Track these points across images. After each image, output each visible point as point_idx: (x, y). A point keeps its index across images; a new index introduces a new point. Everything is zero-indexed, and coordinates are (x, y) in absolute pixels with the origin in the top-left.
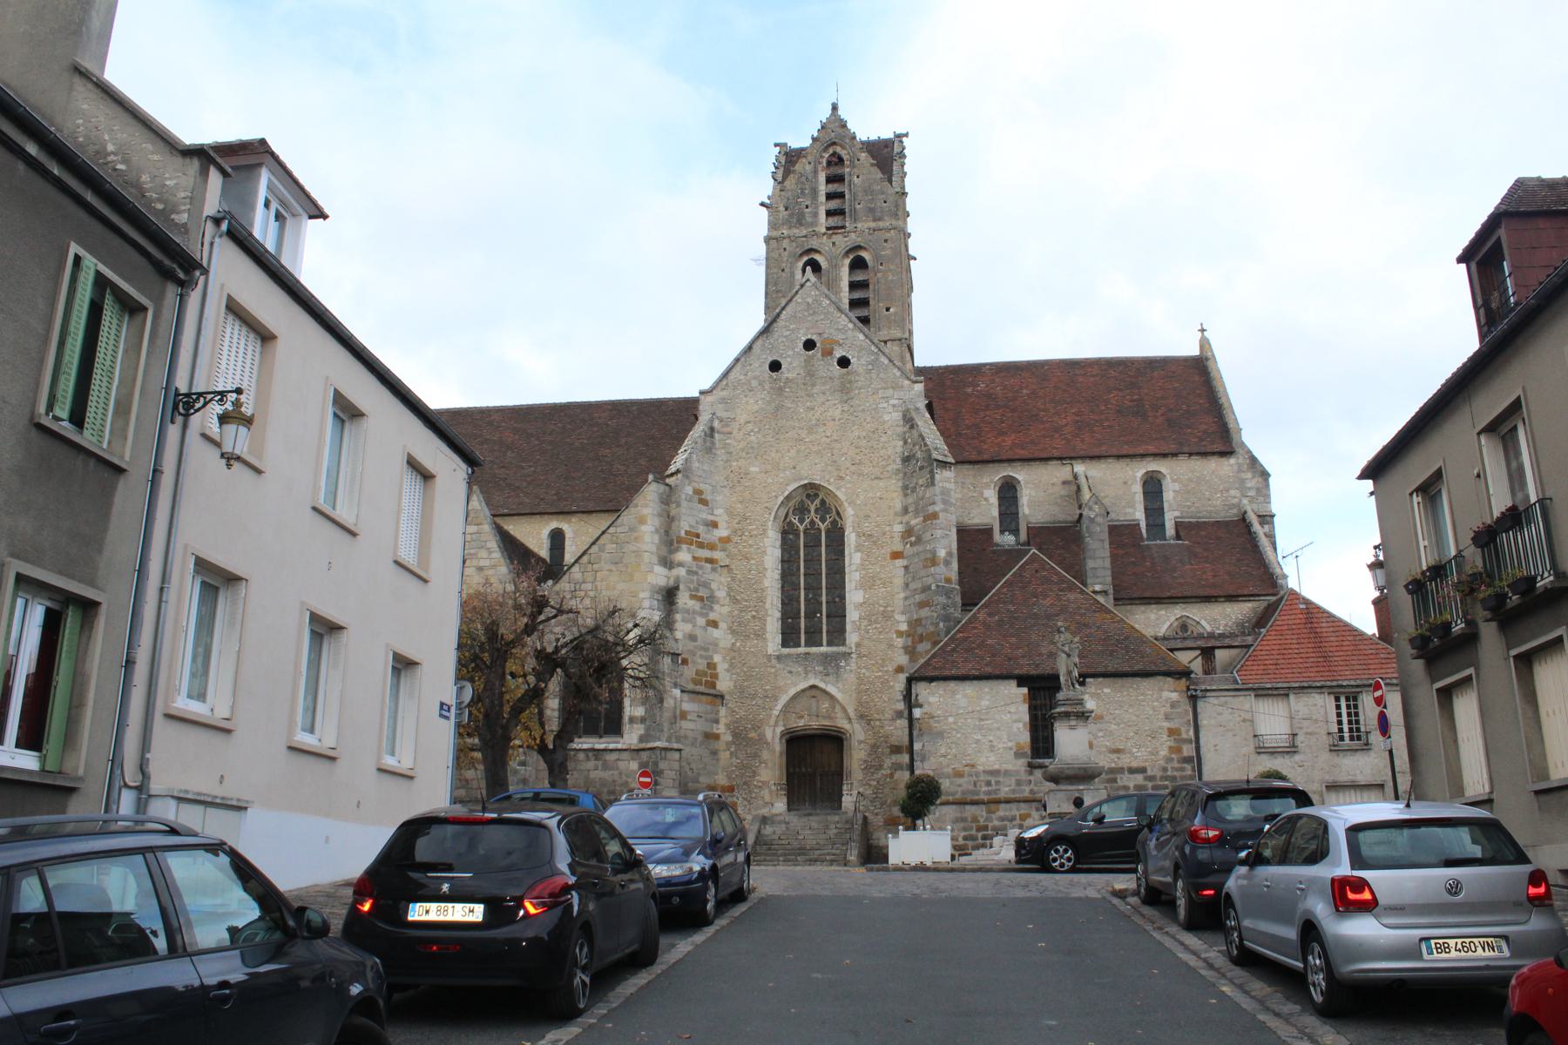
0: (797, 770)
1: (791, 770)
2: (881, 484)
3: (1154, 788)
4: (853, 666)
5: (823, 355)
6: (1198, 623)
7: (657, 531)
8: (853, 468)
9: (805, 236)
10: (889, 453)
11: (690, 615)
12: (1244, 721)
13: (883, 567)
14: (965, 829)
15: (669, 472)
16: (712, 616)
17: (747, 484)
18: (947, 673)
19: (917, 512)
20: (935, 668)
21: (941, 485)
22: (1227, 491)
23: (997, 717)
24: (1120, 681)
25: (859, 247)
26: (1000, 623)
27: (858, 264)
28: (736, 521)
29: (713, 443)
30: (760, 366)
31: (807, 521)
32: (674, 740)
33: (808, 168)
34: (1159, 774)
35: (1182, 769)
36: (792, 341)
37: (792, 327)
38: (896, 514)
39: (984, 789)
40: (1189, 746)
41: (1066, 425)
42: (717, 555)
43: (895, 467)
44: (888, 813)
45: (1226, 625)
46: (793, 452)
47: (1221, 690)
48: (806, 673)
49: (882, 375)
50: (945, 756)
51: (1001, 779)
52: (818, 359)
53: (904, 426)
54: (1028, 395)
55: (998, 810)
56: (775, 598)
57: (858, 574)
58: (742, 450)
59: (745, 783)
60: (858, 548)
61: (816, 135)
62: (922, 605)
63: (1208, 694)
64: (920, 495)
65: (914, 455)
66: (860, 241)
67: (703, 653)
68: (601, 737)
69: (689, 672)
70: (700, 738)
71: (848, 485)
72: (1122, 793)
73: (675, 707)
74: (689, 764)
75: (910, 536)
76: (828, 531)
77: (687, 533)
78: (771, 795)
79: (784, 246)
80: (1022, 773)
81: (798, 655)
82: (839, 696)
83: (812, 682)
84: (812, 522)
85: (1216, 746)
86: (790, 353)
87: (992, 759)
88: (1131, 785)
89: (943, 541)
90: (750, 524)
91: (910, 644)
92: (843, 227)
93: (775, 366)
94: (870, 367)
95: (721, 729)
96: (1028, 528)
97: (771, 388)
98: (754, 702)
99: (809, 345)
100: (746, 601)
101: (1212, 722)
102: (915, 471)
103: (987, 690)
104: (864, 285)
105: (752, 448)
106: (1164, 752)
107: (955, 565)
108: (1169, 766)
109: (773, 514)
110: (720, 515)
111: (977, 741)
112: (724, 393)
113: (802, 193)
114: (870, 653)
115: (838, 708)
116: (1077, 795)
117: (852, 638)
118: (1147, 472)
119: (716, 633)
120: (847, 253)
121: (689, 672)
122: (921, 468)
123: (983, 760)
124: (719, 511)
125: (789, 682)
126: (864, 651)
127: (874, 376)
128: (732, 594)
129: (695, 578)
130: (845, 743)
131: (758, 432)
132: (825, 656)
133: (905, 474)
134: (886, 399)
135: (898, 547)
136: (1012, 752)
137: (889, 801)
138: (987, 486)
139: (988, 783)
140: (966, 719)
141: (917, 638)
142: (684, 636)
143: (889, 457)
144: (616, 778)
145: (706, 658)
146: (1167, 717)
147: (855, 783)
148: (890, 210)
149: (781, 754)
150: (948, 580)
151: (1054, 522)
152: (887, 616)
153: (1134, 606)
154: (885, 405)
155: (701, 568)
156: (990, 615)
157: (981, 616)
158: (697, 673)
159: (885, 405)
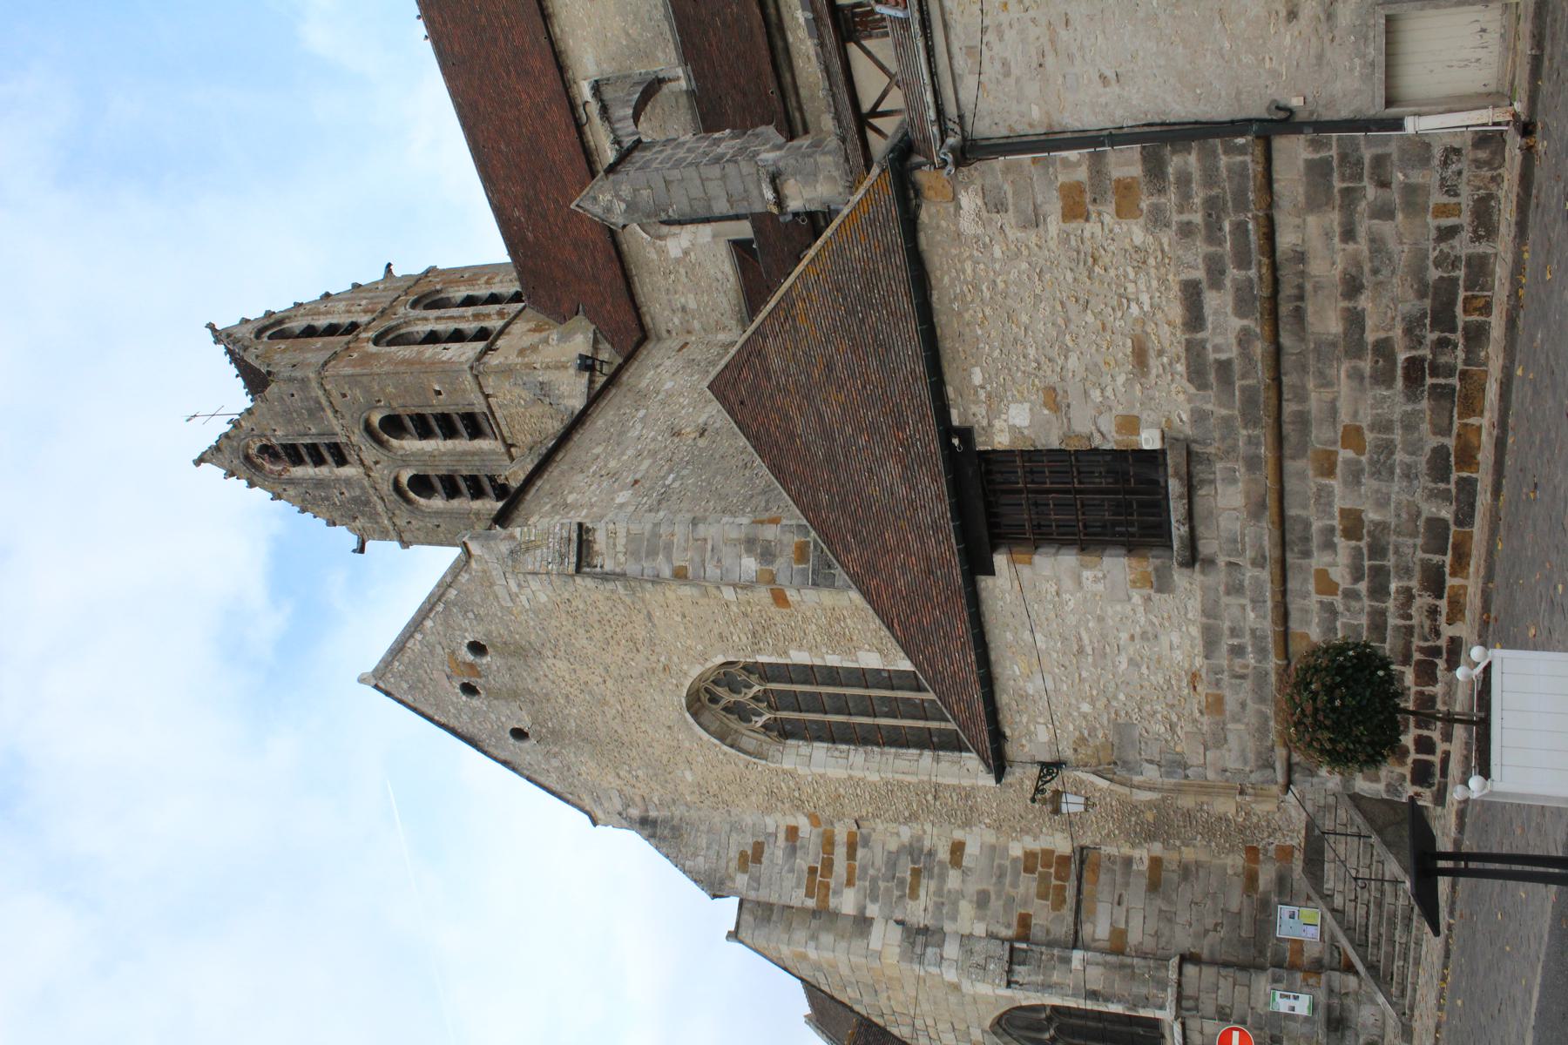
2: (658, 613)
3: (1243, 261)
7: (814, 937)
9: (382, 499)
11: (946, 904)
16: (943, 854)
17: (715, 787)
18: (980, 707)
21: (622, 558)
23: (1072, 620)
24: (947, 345)
25: (368, 428)
27: (394, 425)
28: (779, 804)
29: (665, 821)
30: (528, 753)
32: (1162, 974)
34: (1201, 247)
35: (1184, 180)
38: (706, 594)
39: (1251, 659)
42: (841, 835)
43: (621, 590)
47: (933, 74)
49: (477, 599)
50: (1172, 727)
51: (1226, 625)
52: (488, 682)
56: (901, 764)
61: (244, 483)
63: (951, 110)
67: (1008, 880)
68: (1163, 1036)
69: (1043, 917)
70: (1159, 903)
71: (675, 659)
72: (1259, 348)
73: (1105, 965)
74: (1206, 932)
77: (809, 894)
79: (404, 524)
80: (1210, 580)
84: (755, 698)
85: (1103, 78)
87: (1175, 638)
88: (1237, 323)
89: (727, 562)
93: (519, 734)
94: (471, 615)
95: (1141, 855)
99: (469, 689)
101: (1032, 89)
103: (1009, 636)
106: (1137, 233)
108: (1176, 218)
110: (776, 822)
111: (1131, 661)
113: (327, 499)
119: (972, 849)
120: (381, 443)
121: (1043, 917)
123: (1178, 655)
124: (770, 822)
127: (482, 612)
128: (901, 820)
129: (882, 884)
131: (630, 766)
136: (1156, 597)
138: (662, 251)
139: (1238, 651)
142: (981, 919)
145: (1016, 875)
146: (1035, 220)
153: (799, 82)
155: (864, 869)
158: (1042, 895)
159: (523, 598)
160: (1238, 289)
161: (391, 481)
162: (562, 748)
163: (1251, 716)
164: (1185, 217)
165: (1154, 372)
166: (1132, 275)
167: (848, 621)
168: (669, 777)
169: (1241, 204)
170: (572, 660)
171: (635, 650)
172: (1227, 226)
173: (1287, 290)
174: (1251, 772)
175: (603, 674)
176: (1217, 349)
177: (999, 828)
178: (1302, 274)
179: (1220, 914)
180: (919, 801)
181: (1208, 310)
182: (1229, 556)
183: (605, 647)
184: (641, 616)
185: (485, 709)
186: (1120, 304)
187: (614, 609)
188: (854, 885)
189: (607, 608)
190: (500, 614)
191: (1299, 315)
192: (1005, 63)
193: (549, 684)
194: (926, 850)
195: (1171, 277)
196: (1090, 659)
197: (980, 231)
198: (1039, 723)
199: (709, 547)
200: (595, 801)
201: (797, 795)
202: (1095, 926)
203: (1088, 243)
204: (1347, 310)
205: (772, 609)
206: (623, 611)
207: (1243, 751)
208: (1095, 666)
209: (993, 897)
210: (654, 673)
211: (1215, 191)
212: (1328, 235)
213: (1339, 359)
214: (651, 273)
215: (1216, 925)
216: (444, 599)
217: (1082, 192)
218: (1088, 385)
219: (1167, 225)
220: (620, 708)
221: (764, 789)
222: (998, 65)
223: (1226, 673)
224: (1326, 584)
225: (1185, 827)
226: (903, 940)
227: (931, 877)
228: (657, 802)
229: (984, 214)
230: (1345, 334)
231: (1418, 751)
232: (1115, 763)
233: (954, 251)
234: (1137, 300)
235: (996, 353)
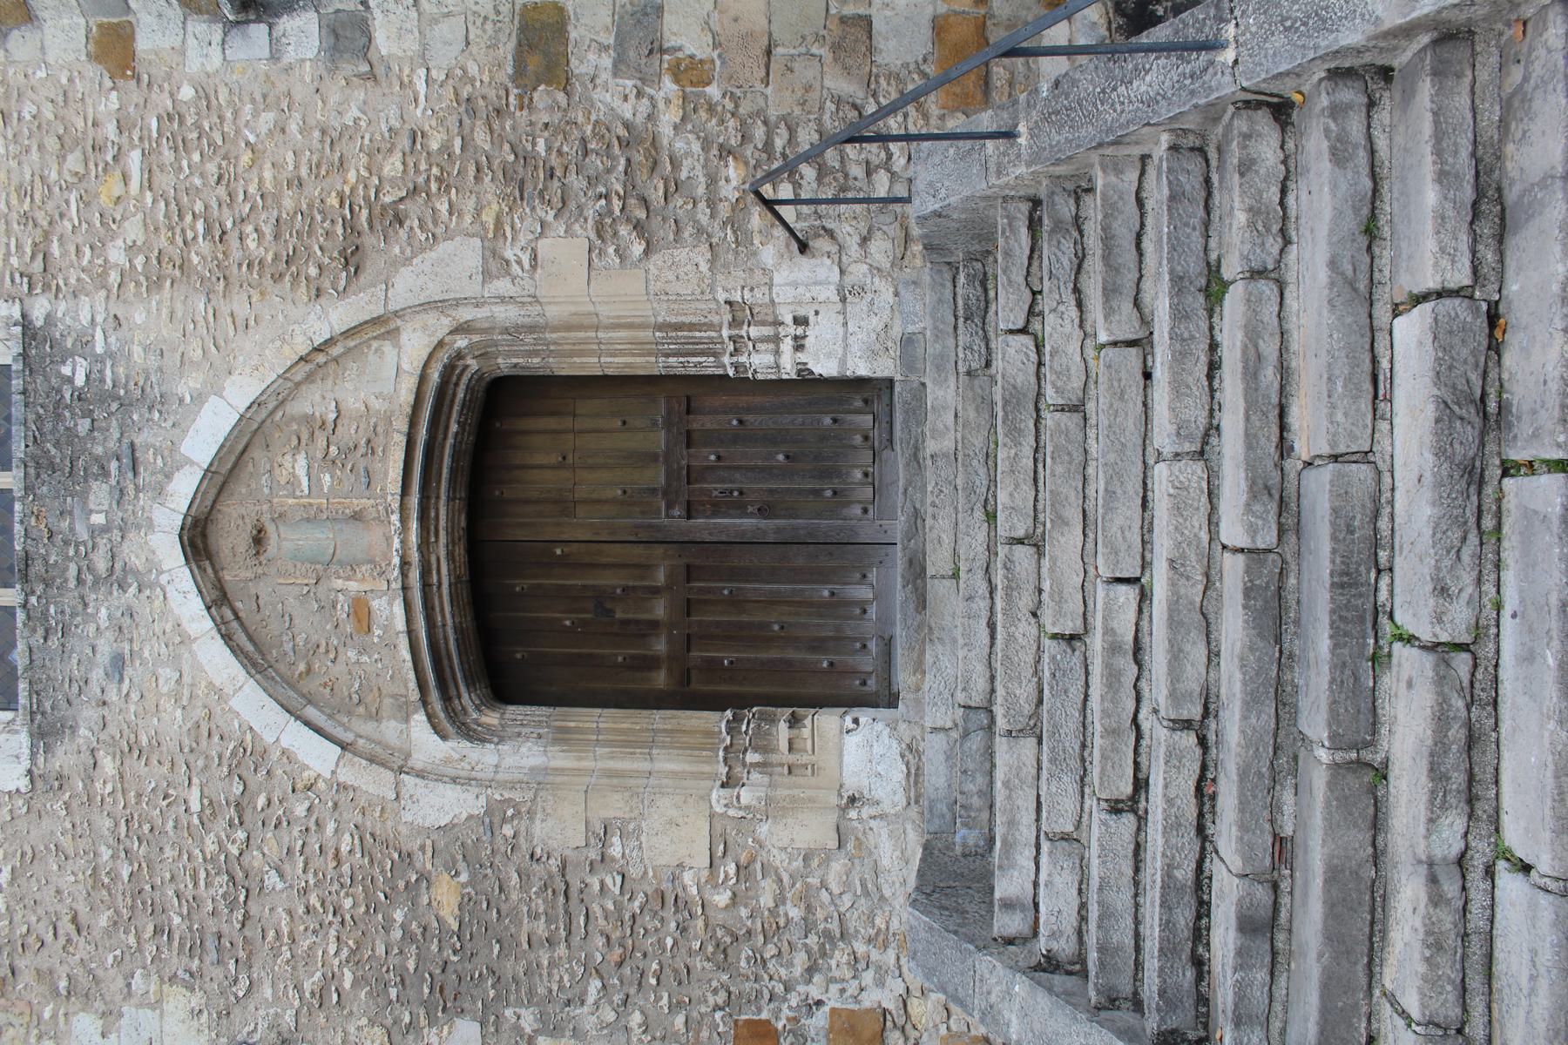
0: (660, 646)
1: (661, 679)
48: (118, 577)
59: (723, 956)
78: (794, 805)
82: (241, 391)
83: (170, 553)
98: (272, 879)
114: (26, 218)
115: (314, 402)
125: (167, 673)
130: (504, 365)
147: (731, 287)
149: (562, 737)
225: (551, 942)
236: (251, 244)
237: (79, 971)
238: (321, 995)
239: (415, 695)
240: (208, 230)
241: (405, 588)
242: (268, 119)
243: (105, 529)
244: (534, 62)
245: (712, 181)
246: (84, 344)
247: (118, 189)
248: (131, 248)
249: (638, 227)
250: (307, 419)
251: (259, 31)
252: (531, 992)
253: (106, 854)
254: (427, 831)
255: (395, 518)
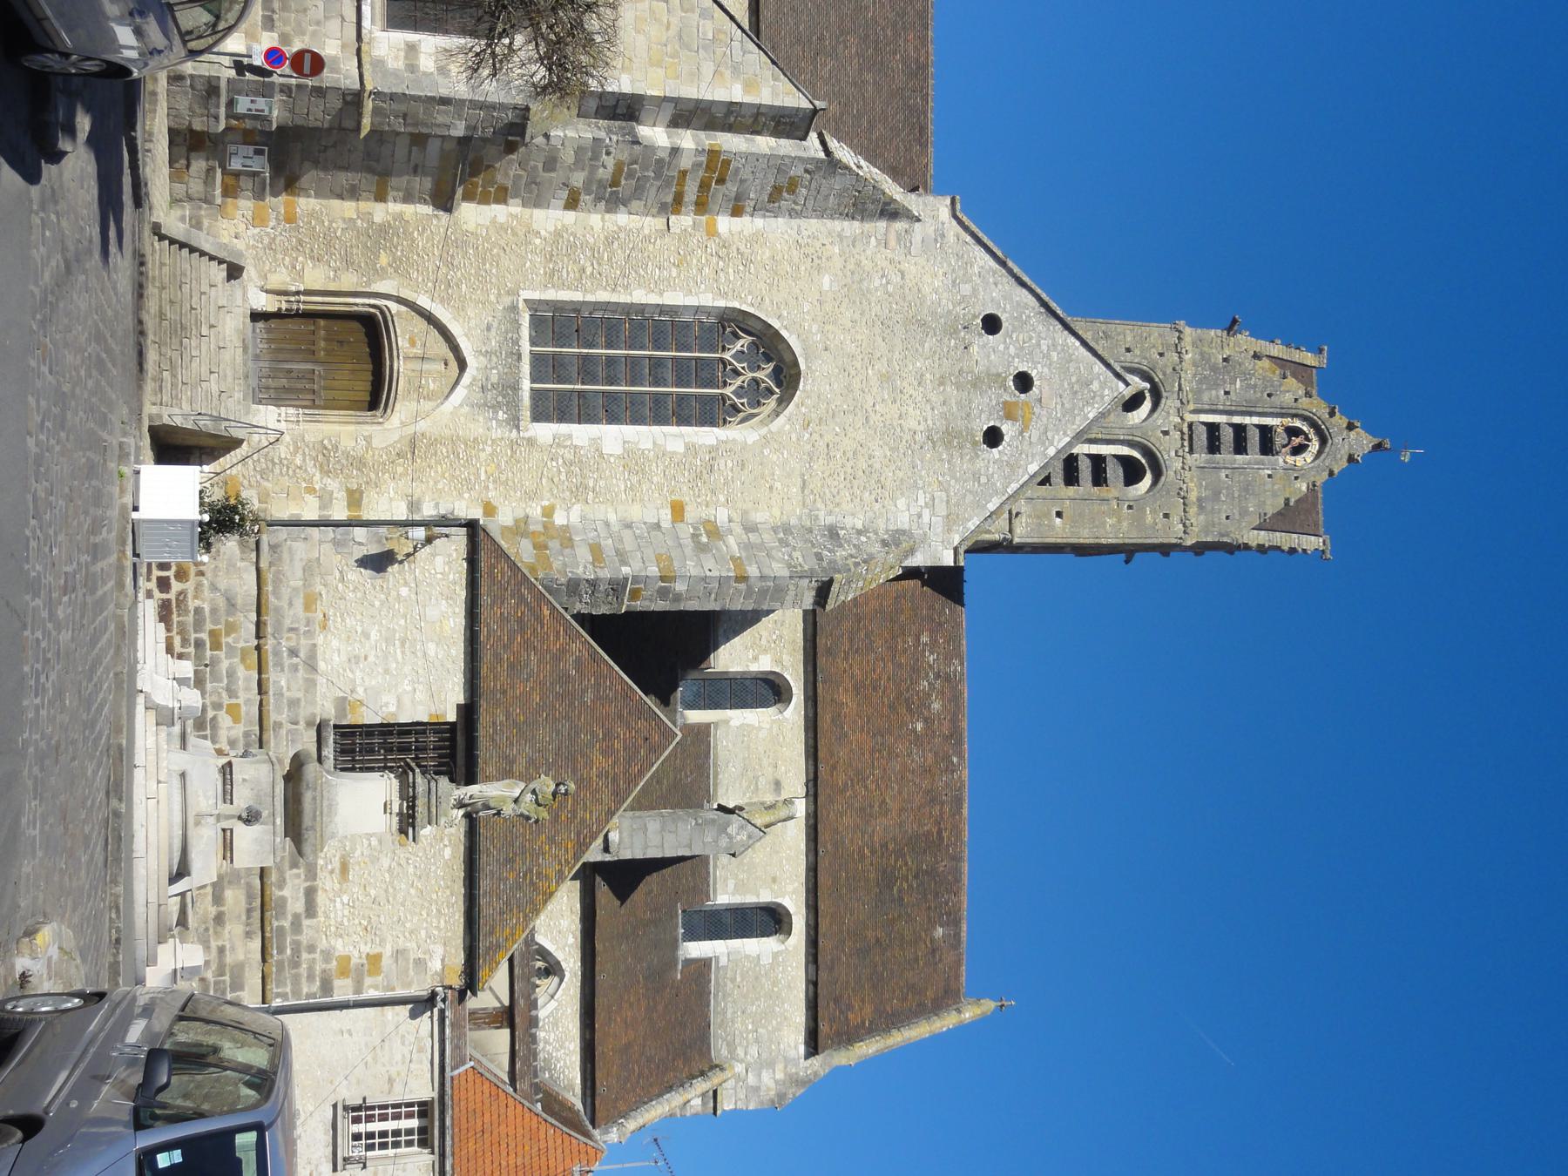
3: (281, 929)
4: (497, 433)
5: (1005, 403)
6: (552, 997)
8: (821, 445)
9: (1180, 389)
10: (844, 506)
12: (391, 1081)
13: (660, 487)
14: (214, 611)
15: (828, 138)
18: (484, 589)
19: (748, 546)
20: (492, 567)
21: (791, 587)
22: (757, 1041)
25: (1158, 474)
26: (565, 678)
28: (742, 248)
31: (739, 366)
33: (1288, 398)
34: (304, 939)
35: (311, 977)
36: (1031, 353)
37: (1054, 355)
38: (745, 513)
40: (351, 990)
41: (866, 787)
43: (822, 514)
44: (246, 483)
45: (547, 1042)
46: (851, 348)
49: (969, 498)
50: (342, 580)
51: (301, 673)
53: (887, 531)
54: (914, 730)
55: (248, 668)
57: (650, 446)
58: (858, 264)
60: (691, 449)
62: (596, 550)
64: (774, 553)
65: (841, 546)
66: (1169, 476)
75: (709, 534)
76: (724, 398)
80: (310, 710)
81: (516, 342)
85: (350, 1033)
86: (1012, 350)
87: (336, 658)
88: (286, 893)
90: (736, 272)
91: (532, 528)
92: (1191, 451)
93: (992, 324)
96: (708, 726)
97: (956, 318)
99: (1024, 382)
100: (610, 259)
102: (813, 545)
104: (1099, 478)
105: (861, 281)
106: (341, 947)
107: (660, 605)
108: (317, 956)
109: (751, 310)
111: (367, 636)
112: (951, 238)
116: (265, 814)
117: (545, 431)
118: (789, 915)
122: (819, 557)
123: (335, 643)
126: (522, 451)
127: (969, 485)
128: (622, 235)
132: (516, 388)
133: (810, 531)
134: (931, 504)
135: (691, 514)
137: (265, 484)
138: (778, 661)
140: (405, 617)
141: (542, 538)
143: (838, 505)
144: (311, 14)
146: (399, 954)
148: (1214, 525)
150: (635, 594)
151: (715, 765)
152: (579, 492)
154: (921, 502)
156: (578, 661)
157: (575, 647)
160: (284, 914)
161: (1159, 409)
162: (949, 312)
163: (285, 592)
164: (312, 956)
165: (337, 858)
166: (345, 919)
167: (623, 488)
168: (849, 280)
169: (280, 964)
170: (899, 430)
171: (831, 446)
172: (289, 951)
173: (257, 914)
174: (286, 540)
175: (872, 414)
176: (298, 876)
177: (531, 232)
178: (248, 925)
179: (321, 159)
180: (599, 264)
181: (303, 900)
182: (296, 730)
183: (859, 448)
184: (811, 486)
185: (1017, 360)
186: (353, 902)
187: (835, 492)
188: (680, 172)
189: (842, 493)
190: (953, 482)
191: (250, 897)
192: (403, 1044)
193: (933, 399)
194: (604, 202)
195: (322, 919)
196: (397, 635)
197: (431, 947)
198: (441, 573)
199: (713, 596)
200: (943, 236)
201: (721, 263)
202: (442, 149)
203: (369, 940)
204: (223, 905)
205: (687, 499)
206: (827, 491)
207: (291, 560)
208: (394, 629)
209: (540, 166)
210: (821, 419)
211: (293, 971)
212: (233, 949)
213: (227, 873)
214: (794, 641)
215: (325, 151)
216: (1004, 498)
217: (369, 971)
218: (379, 848)
219: (322, 951)
220: (870, 372)
221: (752, 270)
222: (407, 1043)
223: (302, 632)
224: (233, 711)
225: (351, 246)
226: (639, 110)
227: (600, 181)
228: (873, 238)
229: (427, 957)
230: (223, 891)
231: (168, 578)
232: (387, 539)
233: (449, 934)
234: (343, 904)
235: (433, 868)
236: (444, 450)
237: (504, 236)
238: (424, 229)
239: (395, 319)
240: (458, 454)
241: (398, 350)
242: (440, 486)
243: (493, 368)
244: (357, 495)
245: (304, 460)
246: (497, 420)
247: (489, 468)
248: (484, 450)
249: (326, 448)
250: (429, 400)
251: (443, 512)
252: (358, 232)
253: (494, 271)
254: (390, 278)
255: (401, 370)
